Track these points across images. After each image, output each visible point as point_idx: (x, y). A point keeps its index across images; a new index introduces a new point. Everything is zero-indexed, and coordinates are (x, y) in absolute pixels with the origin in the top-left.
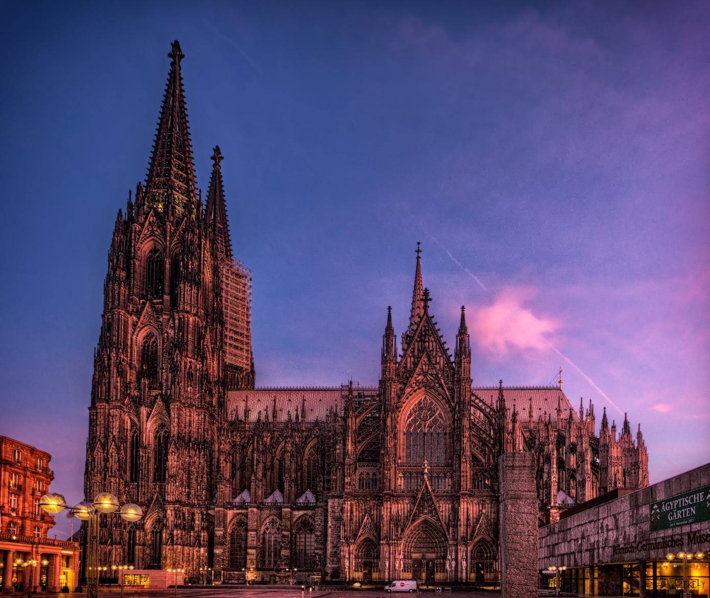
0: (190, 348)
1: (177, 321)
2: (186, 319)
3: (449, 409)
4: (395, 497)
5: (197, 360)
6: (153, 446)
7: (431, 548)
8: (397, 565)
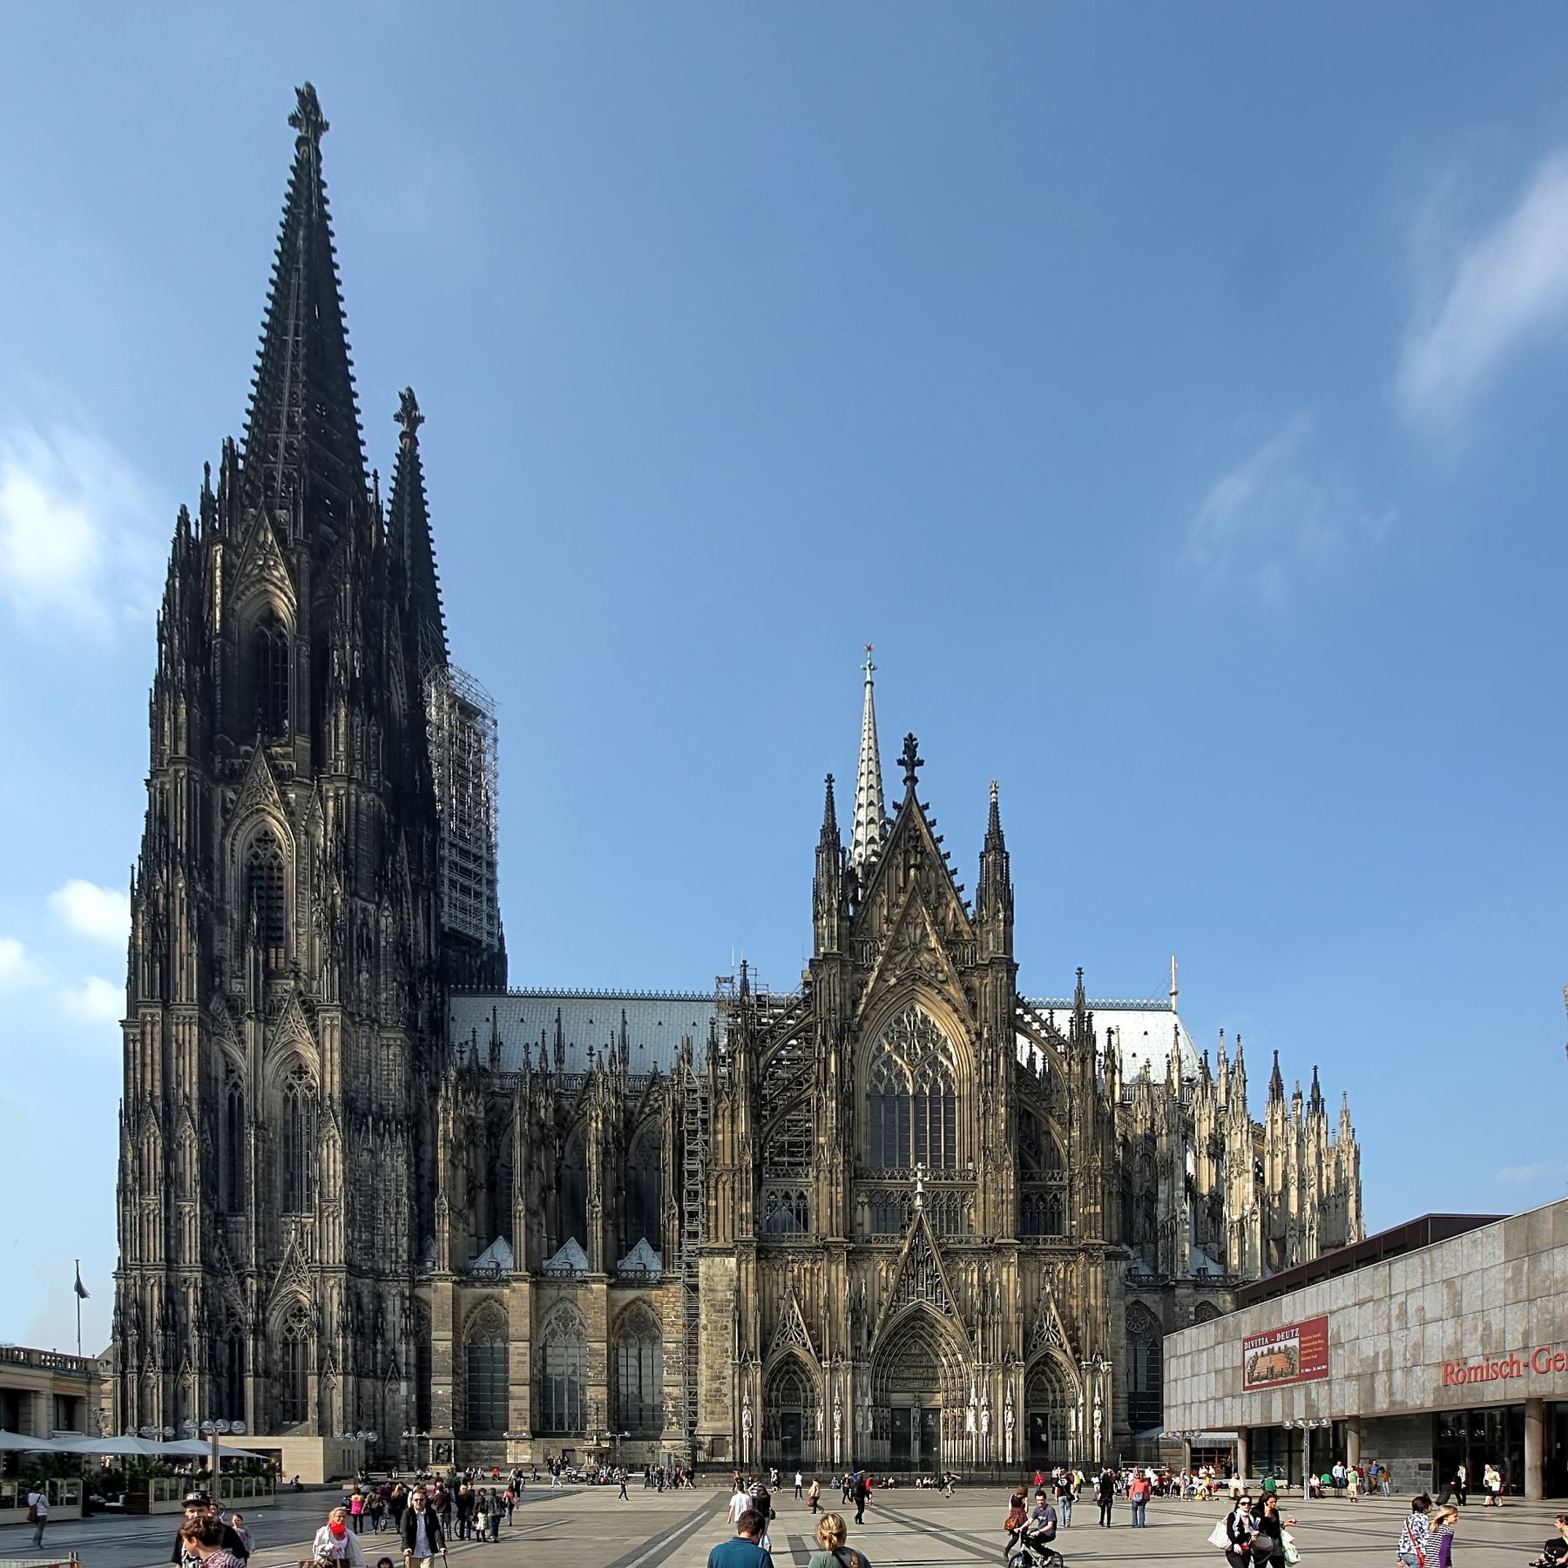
0: (364, 873)
1: (331, 804)
2: (353, 798)
3: (966, 1038)
5: (378, 905)
6: (280, 1122)
8: (860, 1422)
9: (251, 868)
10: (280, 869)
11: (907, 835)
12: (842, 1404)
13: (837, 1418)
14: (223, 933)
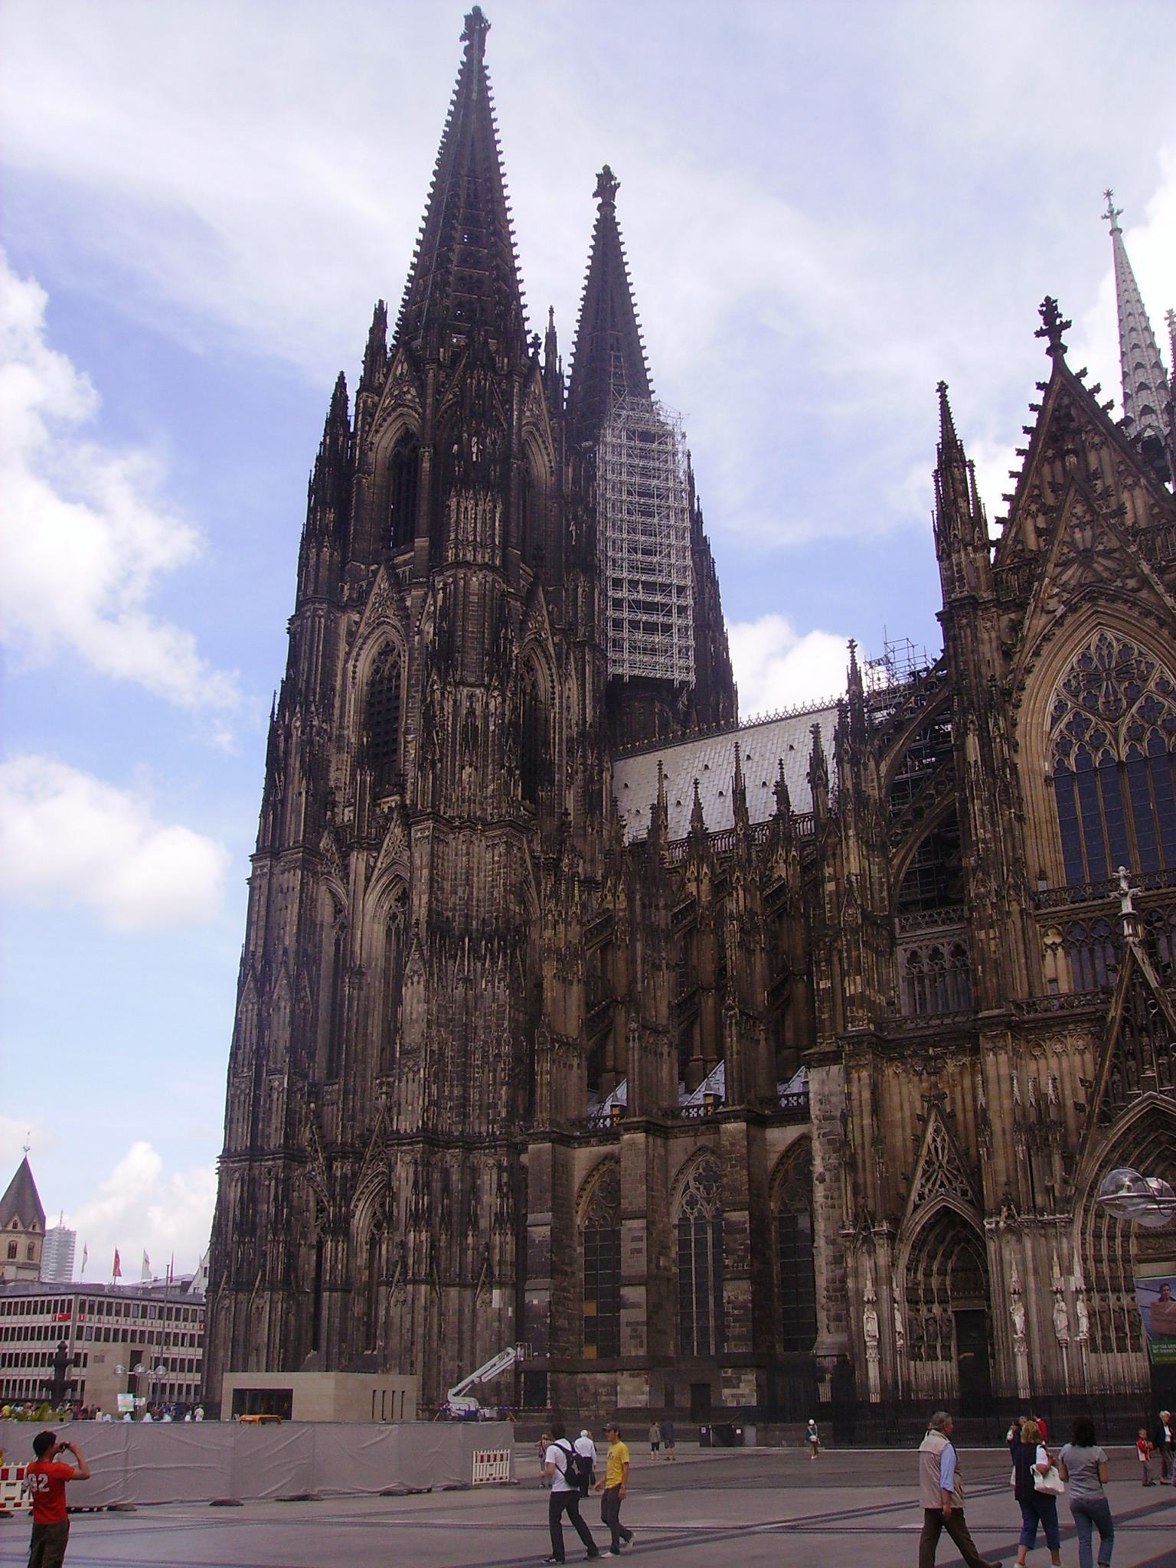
0: (472, 657)
4: (1031, 1026)
9: (371, 684)
10: (398, 676)
12: (1022, 1294)
13: (1018, 1320)
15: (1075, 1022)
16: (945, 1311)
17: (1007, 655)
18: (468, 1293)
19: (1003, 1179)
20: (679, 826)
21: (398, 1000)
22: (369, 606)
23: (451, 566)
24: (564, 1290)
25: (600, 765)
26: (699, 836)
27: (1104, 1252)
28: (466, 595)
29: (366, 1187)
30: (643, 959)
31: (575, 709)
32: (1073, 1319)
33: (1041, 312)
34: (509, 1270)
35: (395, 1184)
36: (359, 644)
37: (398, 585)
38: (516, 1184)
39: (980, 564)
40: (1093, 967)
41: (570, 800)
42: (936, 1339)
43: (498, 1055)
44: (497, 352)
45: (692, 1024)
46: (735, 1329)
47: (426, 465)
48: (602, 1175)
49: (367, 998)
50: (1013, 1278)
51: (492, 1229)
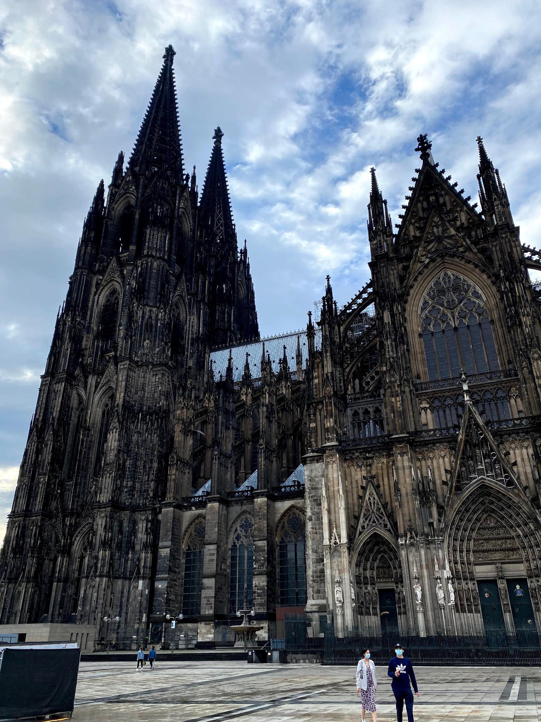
0: (152, 295)
3: (489, 281)
4: (418, 443)
7: (513, 550)
9: (105, 306)
10: (118, 304)
11: (430, 183)
12: (419, 578)
13: (419, 593)
14: (88, 337)
15: (440, 443)
16: (374, 589)
17: (402, 279)
18: (127, 582)
19: (407, 518)
20: (237, 375)
21: (106, 440)
22: (107, 273)
23: (145, 256)
24: (174, 580)
25: (205, 351)
26: (247, 376)
27: (458, 558)
28: (151, 268)
29: (82, 530)
30: (222, 423)
31: (195, 327)
32: (446, 594)
33: (418, 141)
34: (148, 571)
35: (95, 527)
36: (101, 288)
37: (121, 264)
38: (154, 529)
39: (389, 242)
40: (446, 418)
41: (191, 363)
42: (370, 604)
43: (151, 468)
44: (171, 176)
45: (241, 456)
46: (258, 600)
47: (137, 216)
48: (196, 524)
49: (91, 441)
50: (415, 570)
51: (141, 550)
